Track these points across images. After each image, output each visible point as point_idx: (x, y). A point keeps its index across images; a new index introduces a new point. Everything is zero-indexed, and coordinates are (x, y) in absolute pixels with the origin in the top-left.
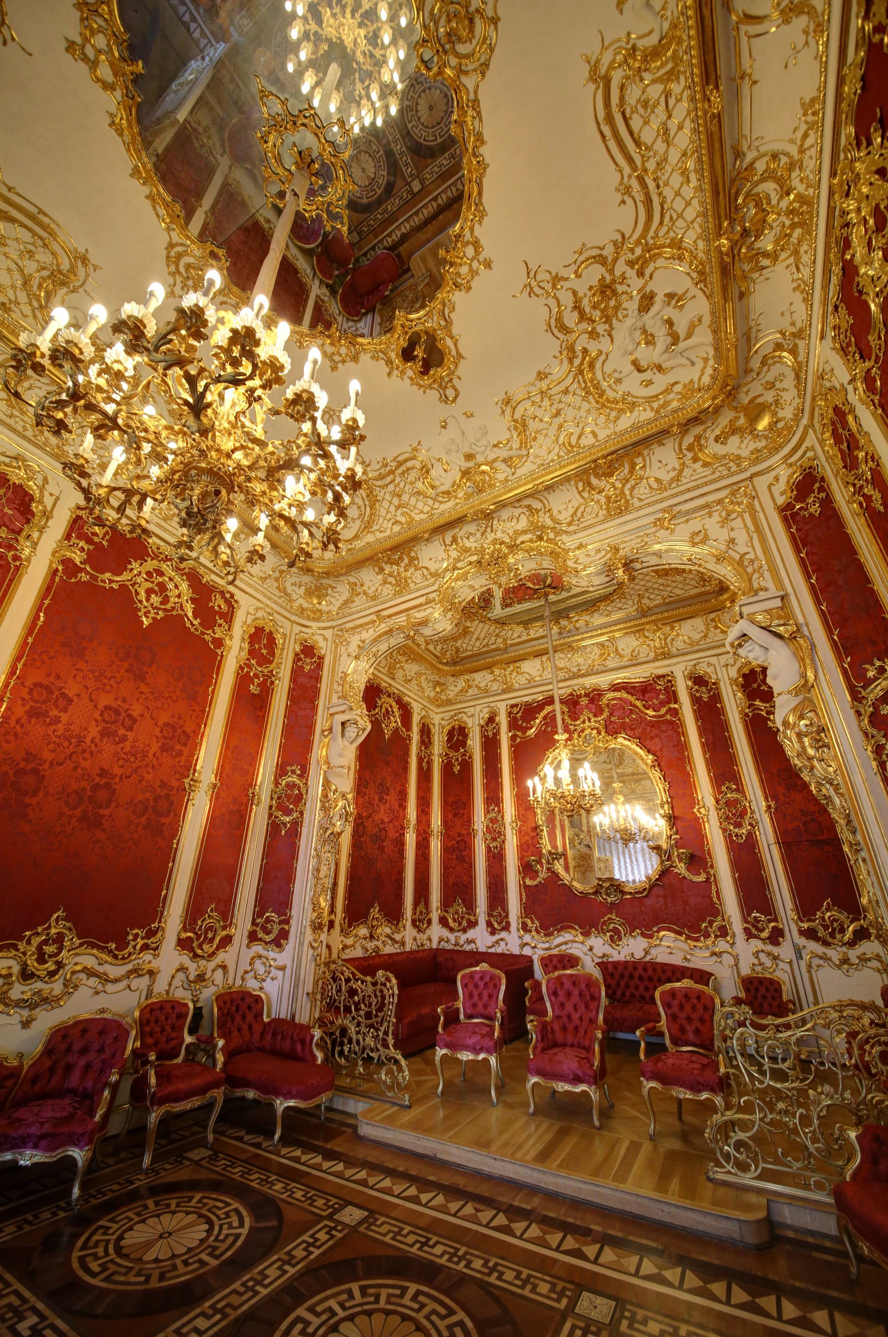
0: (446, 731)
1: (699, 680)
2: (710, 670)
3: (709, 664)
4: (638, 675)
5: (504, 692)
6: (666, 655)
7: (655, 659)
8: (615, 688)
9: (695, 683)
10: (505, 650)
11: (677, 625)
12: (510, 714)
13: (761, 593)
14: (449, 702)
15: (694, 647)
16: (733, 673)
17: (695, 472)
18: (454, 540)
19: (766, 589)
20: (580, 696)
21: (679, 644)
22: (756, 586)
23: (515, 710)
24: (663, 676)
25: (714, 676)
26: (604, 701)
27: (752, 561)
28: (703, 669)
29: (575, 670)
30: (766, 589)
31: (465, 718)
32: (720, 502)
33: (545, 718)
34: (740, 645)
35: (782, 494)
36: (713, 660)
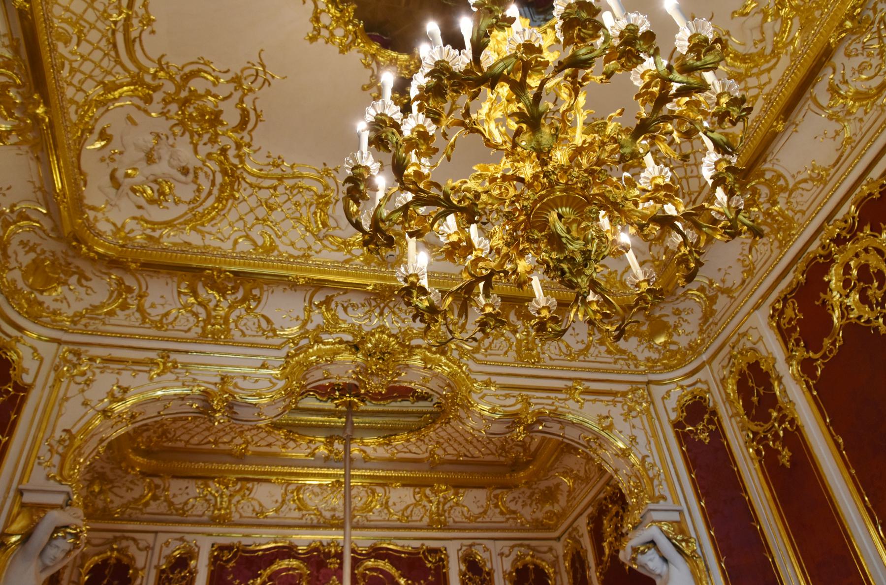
0: (89, 564)
1: (473, 566)
2: (486, 555)
3: (486, 549)
4: (404, 542)
5: (215, 521)
6: (445, 527)
7: (429, 527)
8: (377, 553)
9: (469, 568)
10: (241, 458)
11: (461, 491)
12: (215, 560)
13: (662, 502)
14: (106, 514)
15: (473, 523)
16: (508, 565)
17: (599, 353)
18: (327, 302)
19: (664, 498)
20: (328, 555)
21: (456, 515)
22: (657, 494)
23: (227, 555)
24: (434, 551)
25: (489, 565)
26: (361, 569)
27: (653, 465)
28: (480, 555)
29: (328, 515)
30: (664, 498)
31: (133, 550)
32: (624, 394)
33: (270, 578)
34: (643, 553)
35: (674, 410)
36: (489, 544)
